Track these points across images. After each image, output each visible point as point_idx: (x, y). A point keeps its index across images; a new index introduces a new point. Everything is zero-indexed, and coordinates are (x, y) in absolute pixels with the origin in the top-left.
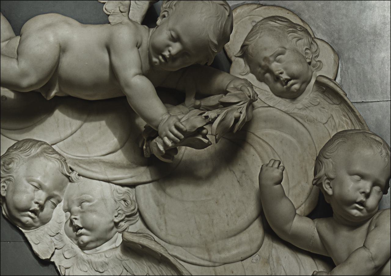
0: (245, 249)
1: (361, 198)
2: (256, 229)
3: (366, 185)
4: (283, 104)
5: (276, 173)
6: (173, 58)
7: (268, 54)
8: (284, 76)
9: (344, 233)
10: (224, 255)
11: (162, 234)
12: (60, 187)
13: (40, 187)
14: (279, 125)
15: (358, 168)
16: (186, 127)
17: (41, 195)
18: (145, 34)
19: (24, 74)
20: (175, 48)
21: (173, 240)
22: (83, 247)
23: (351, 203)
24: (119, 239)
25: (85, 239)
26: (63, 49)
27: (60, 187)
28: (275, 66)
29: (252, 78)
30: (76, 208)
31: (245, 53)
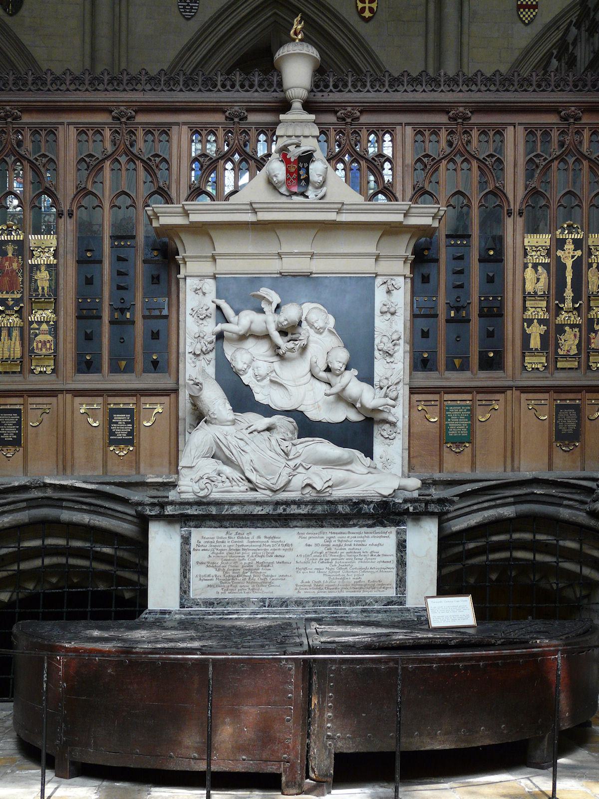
0: (306, 381)
1: (339, 368)
2: (309, 374)
3: (341, 365)
4: (318, 336)
5: (315, 360)
6: (285, 325)
7: (313, 321)
8: (318, 328)
9: (334, 377)
10: (300, 383)
11: (281, 376)
12: (251, 363)
13: (245, 363)
14: (316, 342)
15: (339, 360)
16: (289, 347)
17: (245, 366)
18: (276, 317)
19: (241, 331)
20: (286, 323)
21: (285, 379)
22: (258, 381)
23: (336, 370)
24: (268, 378)
25: (258, 379)
26: (252, 322)
27: (251, 363)
28: (316, 325)
29: (308, 327)
30: (256, 370)
31: (306, 319)
